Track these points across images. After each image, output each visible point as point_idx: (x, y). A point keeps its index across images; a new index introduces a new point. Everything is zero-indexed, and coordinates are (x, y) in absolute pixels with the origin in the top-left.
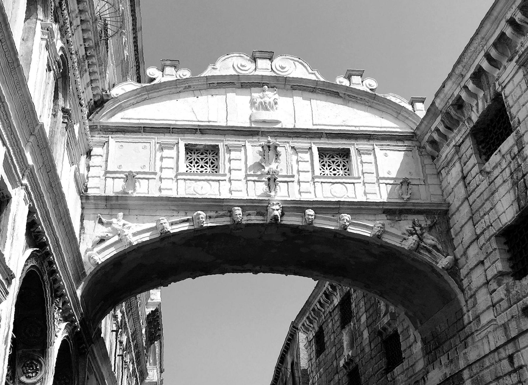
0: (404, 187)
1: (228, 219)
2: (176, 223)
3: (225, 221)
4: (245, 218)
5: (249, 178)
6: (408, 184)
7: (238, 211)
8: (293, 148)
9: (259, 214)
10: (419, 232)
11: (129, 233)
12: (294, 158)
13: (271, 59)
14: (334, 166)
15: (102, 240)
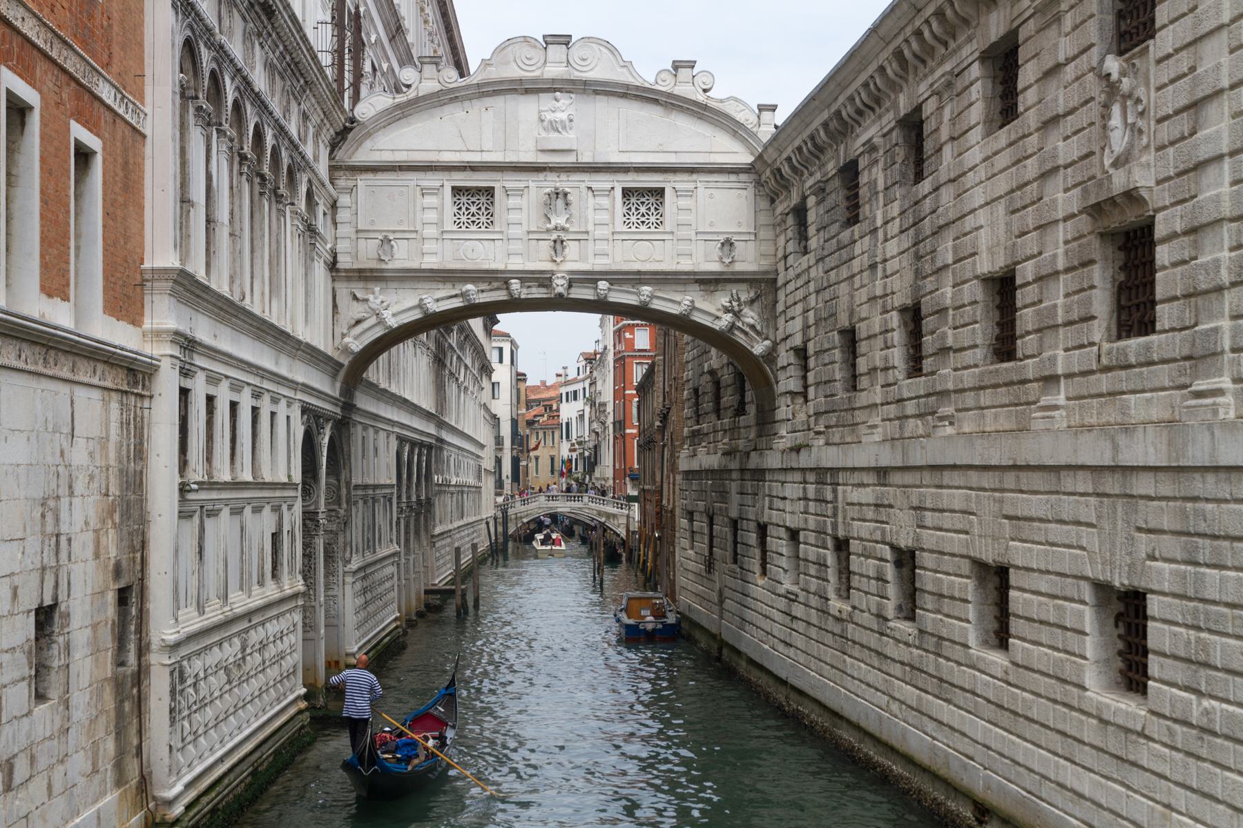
0: (726, 248)
1: (504, 292)
2: (442, 299)
3: (500, 296)
4: (525, 291)
5: (532, 236)
6: (731, 244)
7: (515, 285)
8: (590, 188)
9: (539, 286)
10: (736, 309)
11: (387, 314)
12: (591, 199)
13: (567, 44)
14: (643, 209)
15: (358, 322)
